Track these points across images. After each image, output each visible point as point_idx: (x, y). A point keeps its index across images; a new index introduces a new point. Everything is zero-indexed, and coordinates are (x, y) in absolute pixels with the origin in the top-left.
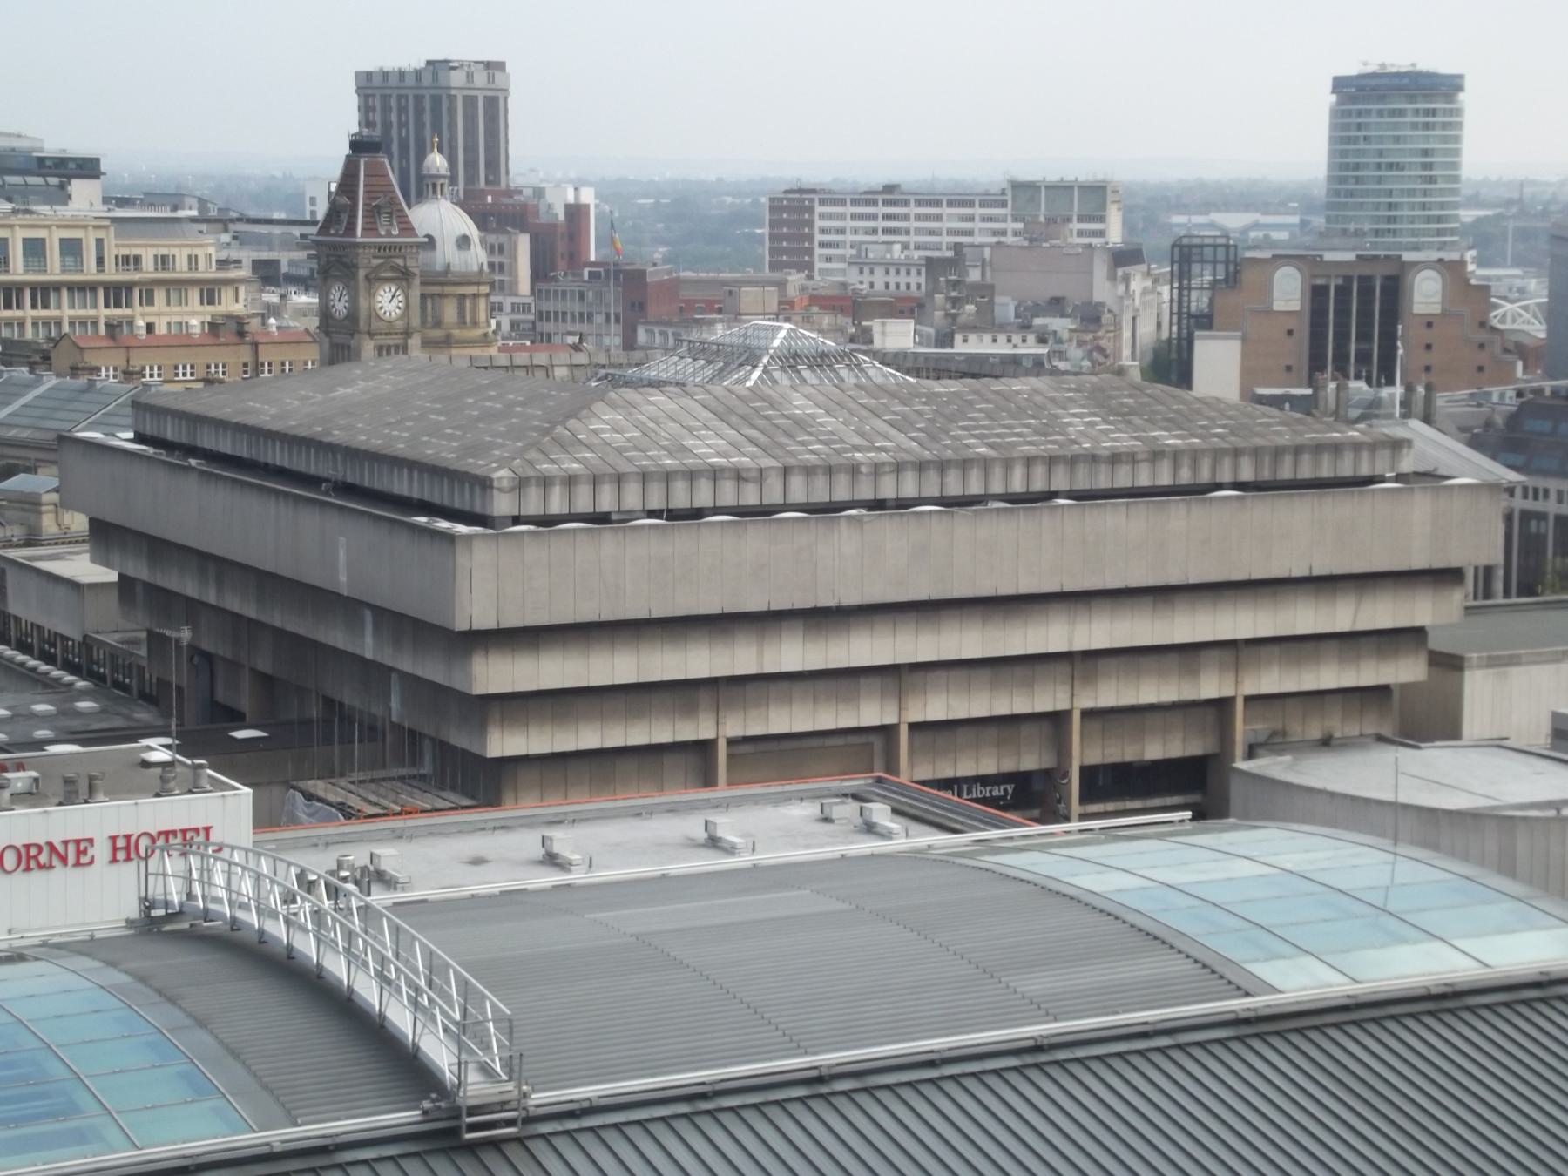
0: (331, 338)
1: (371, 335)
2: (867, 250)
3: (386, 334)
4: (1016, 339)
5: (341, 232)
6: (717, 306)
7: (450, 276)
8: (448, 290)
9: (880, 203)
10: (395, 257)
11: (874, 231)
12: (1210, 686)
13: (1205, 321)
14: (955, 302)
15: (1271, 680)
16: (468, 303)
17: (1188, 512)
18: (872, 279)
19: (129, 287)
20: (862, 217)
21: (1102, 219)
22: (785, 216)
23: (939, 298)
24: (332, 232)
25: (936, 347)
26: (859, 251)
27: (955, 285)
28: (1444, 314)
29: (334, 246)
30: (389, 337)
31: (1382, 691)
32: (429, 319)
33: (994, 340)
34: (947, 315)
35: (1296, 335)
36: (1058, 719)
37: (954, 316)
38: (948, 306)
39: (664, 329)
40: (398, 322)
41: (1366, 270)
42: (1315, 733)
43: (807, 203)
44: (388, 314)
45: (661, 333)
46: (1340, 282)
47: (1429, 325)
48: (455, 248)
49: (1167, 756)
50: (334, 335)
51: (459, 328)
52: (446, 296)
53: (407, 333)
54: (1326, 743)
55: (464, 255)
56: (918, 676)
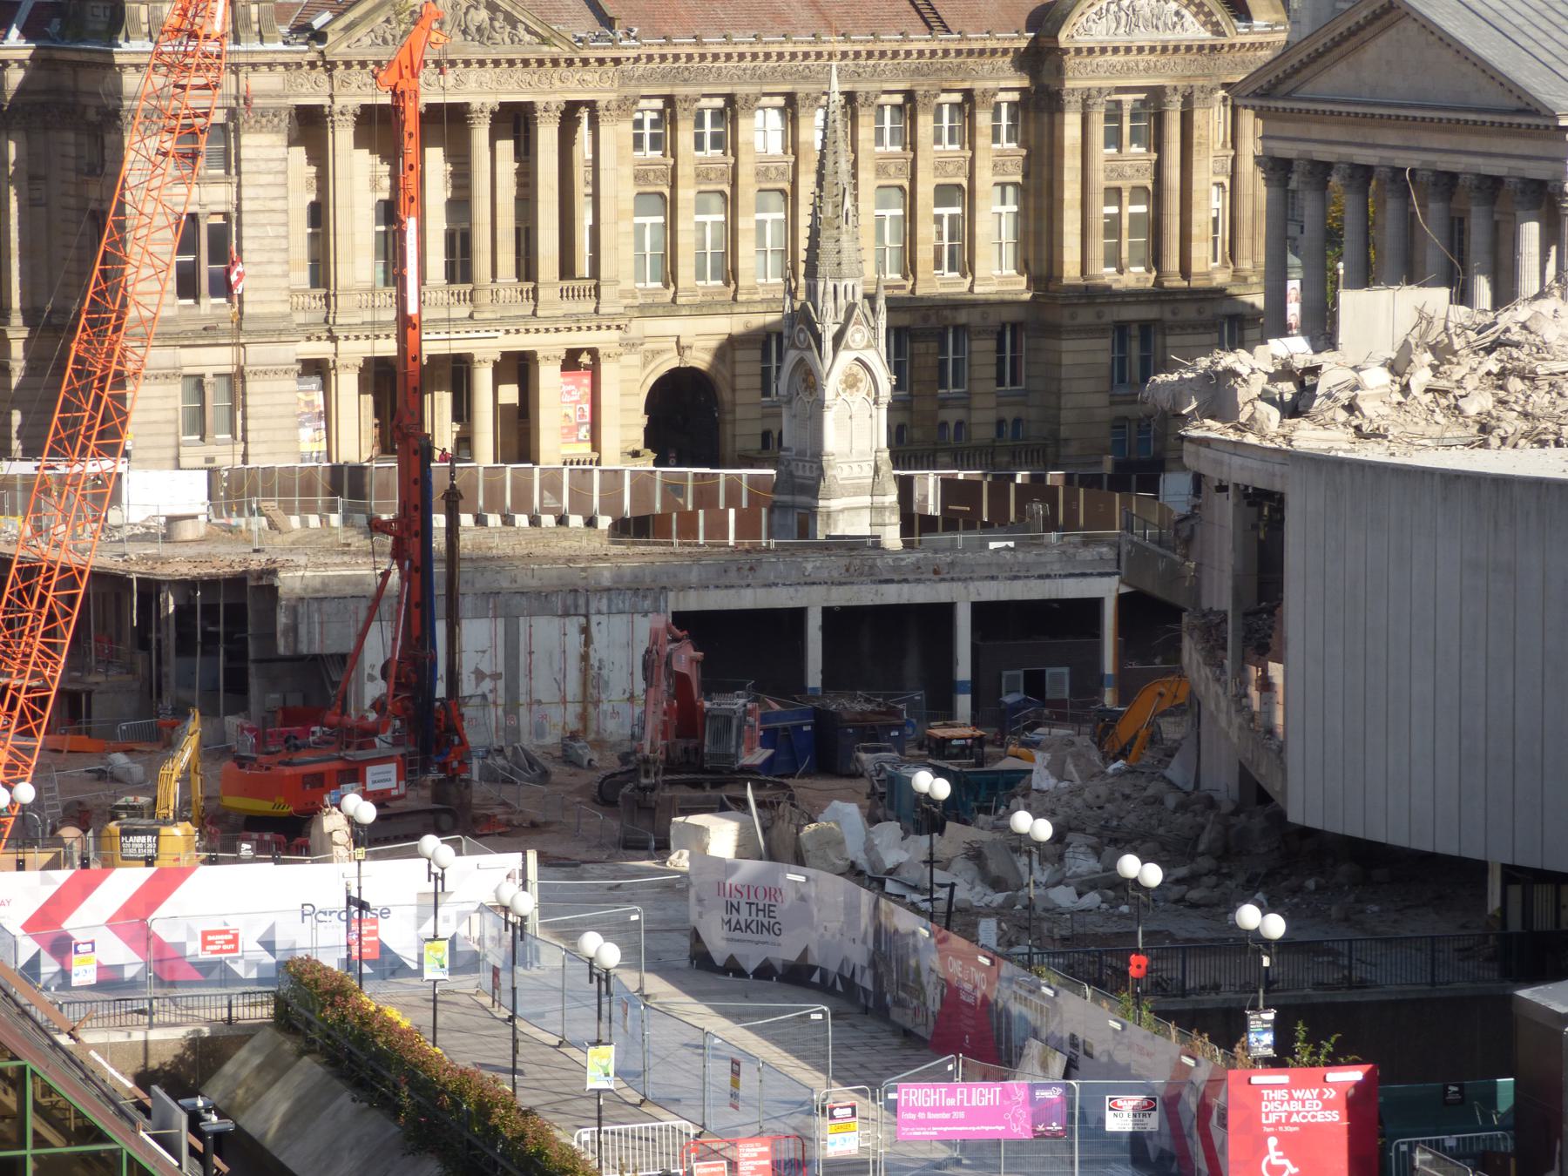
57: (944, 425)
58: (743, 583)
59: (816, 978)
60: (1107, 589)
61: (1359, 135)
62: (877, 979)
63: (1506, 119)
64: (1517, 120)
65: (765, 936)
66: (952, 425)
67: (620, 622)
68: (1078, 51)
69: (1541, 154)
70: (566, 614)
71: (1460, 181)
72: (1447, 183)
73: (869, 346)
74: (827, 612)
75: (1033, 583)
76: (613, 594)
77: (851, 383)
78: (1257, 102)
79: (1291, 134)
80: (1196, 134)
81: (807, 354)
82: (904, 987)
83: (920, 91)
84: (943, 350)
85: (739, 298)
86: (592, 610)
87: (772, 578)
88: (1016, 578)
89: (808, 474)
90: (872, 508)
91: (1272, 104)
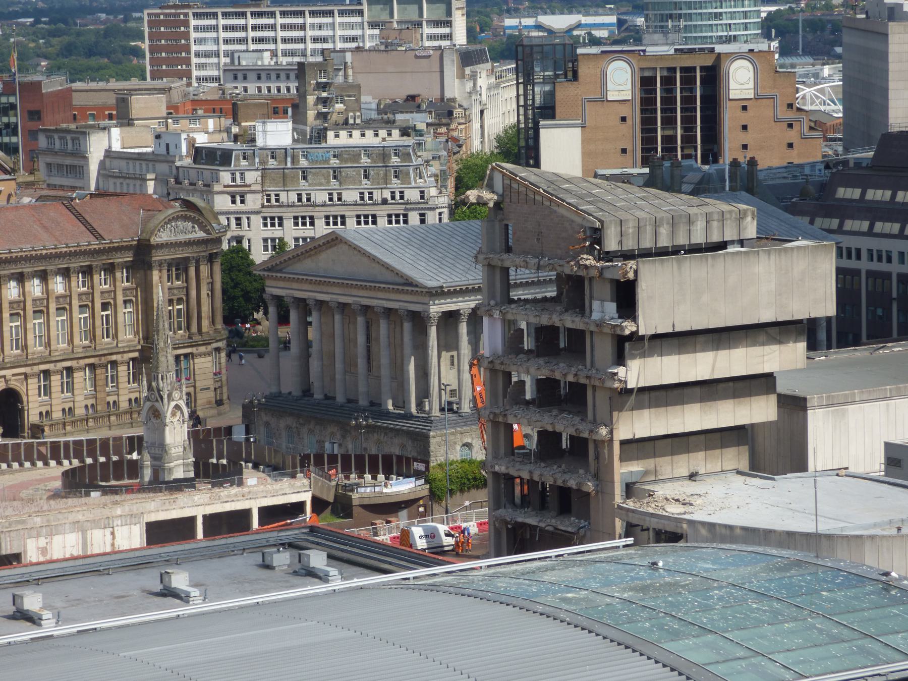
2: (239, 57)
4: (383, 133)
6: (107, 113)
9: (249, 15)
11: (244, 41)
13: (548, 111)
20: (232, 28)
21: (449, 23)
22: (162, 29)
27: (324, 87)
28: (757, 98)
33: (363, 135)
35: (629, 121)
41: (687, 62)
43: (182, 17)
45: (60, 138)
46: (665, 73)
47: (744, 108)
57: (108, 403)
58: (172, 507)
60: (307, 497)
61: (319, 288)
63: (400, 288)
64: (406, 288)
66: (111, 403)
67: (126, 528)
68: (157, 244)
69: (416, 301)
70: (105, 528)
71: (375, 310)
72: (366, 309)
73: (180, 399)
74: (204, 516)
75: (280, 497)
76: (123, 517)
77: (173, 414)
78: (266, 273)
79: (282, 286)
80: (201, 275)
81: (156, 404)
83: (94, 264)
84: (107, 372)
85: (29, 357)
86: (115, 525)
87: (182, 505)
88: (274, 496)
89: (157, 452)
90: (184, 464)
91: (274, 274)
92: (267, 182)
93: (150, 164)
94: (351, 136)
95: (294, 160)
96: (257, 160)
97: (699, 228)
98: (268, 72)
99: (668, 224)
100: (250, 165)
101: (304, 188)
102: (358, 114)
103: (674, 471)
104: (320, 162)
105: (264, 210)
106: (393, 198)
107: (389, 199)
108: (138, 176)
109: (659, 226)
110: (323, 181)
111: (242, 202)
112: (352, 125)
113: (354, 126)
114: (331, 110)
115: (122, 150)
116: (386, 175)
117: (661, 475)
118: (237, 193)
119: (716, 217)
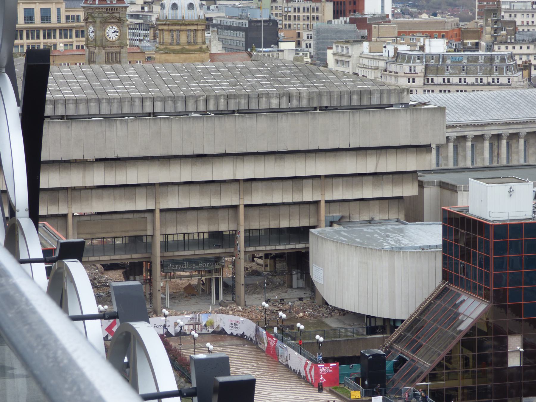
0: (89, 49)
1: (104, 48)
3: (111, 47)
5: (91, 2)
6: (441, 34)
7: (183, 21)
8: (183, 28)
10: (115, 13)
12: (308, 196)
14: (496, 30)
15: (339, 194)
16: (192, 34)
17: (287, 119)
18: (533, 20)
19: (71, 29)
23: (488, 29)
24: (88, 2)
25: (487, 51)
26: (510, 6)
27: (496, 22)
29: (89, 8)
30: (113, 48)
31: (401, 198)
32: (175, 41)
33: (521, 48)
34: (493, 36)
36: (235, 207)
37: (495, 37)
38: (493, 32)
39: (343, 45)
40: (116, 42)
42: (366, 218)
44: (111, 38)
48: (187, 8)
49: (291, 226)
50: (90, 48)
51: (188, 45)
52: (182, 30)
53: (122, 46)
54: (371, 222)
55: (191, 12)
56: (164, 189)
59: (245, 337)
62: (256, 339)
65: (237, 329)
82: (261, 341)
92: (428, 71)
93: (377, 61)
94: (507, 48)
95: (444, 60)
96: (424, 60)
97: (376, 97)
98: (527, 13)
99: (357, 94)
100: (420, 63)
101: (447, 75)
102: (513, 37)
103: (361, 218)
104: (457, 62)
105: (425, 86)
106: (493, 82)
107: (491, 82)
108: (370, 67)
109: (352, 95)
110: (457, 72)
111: (414, 82)
112: (509, 43)
113: (511, 43)
114: (499, 34)
115: (368, 54)
116: (491, 69)
117: (353, 219)
118: (411, 77)
119: (386, 92)
